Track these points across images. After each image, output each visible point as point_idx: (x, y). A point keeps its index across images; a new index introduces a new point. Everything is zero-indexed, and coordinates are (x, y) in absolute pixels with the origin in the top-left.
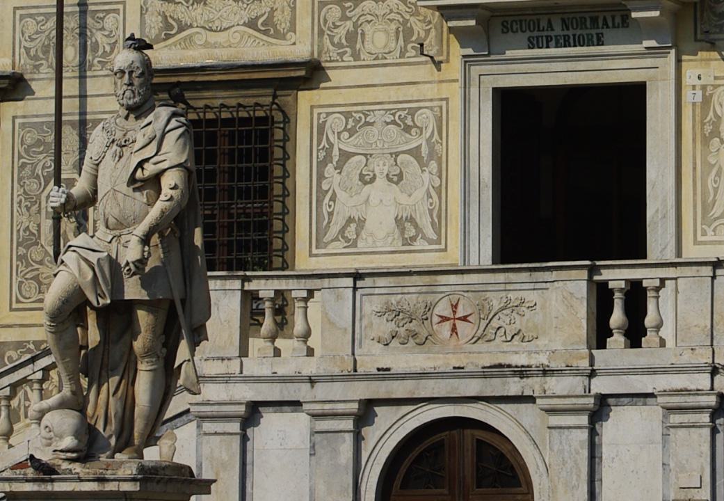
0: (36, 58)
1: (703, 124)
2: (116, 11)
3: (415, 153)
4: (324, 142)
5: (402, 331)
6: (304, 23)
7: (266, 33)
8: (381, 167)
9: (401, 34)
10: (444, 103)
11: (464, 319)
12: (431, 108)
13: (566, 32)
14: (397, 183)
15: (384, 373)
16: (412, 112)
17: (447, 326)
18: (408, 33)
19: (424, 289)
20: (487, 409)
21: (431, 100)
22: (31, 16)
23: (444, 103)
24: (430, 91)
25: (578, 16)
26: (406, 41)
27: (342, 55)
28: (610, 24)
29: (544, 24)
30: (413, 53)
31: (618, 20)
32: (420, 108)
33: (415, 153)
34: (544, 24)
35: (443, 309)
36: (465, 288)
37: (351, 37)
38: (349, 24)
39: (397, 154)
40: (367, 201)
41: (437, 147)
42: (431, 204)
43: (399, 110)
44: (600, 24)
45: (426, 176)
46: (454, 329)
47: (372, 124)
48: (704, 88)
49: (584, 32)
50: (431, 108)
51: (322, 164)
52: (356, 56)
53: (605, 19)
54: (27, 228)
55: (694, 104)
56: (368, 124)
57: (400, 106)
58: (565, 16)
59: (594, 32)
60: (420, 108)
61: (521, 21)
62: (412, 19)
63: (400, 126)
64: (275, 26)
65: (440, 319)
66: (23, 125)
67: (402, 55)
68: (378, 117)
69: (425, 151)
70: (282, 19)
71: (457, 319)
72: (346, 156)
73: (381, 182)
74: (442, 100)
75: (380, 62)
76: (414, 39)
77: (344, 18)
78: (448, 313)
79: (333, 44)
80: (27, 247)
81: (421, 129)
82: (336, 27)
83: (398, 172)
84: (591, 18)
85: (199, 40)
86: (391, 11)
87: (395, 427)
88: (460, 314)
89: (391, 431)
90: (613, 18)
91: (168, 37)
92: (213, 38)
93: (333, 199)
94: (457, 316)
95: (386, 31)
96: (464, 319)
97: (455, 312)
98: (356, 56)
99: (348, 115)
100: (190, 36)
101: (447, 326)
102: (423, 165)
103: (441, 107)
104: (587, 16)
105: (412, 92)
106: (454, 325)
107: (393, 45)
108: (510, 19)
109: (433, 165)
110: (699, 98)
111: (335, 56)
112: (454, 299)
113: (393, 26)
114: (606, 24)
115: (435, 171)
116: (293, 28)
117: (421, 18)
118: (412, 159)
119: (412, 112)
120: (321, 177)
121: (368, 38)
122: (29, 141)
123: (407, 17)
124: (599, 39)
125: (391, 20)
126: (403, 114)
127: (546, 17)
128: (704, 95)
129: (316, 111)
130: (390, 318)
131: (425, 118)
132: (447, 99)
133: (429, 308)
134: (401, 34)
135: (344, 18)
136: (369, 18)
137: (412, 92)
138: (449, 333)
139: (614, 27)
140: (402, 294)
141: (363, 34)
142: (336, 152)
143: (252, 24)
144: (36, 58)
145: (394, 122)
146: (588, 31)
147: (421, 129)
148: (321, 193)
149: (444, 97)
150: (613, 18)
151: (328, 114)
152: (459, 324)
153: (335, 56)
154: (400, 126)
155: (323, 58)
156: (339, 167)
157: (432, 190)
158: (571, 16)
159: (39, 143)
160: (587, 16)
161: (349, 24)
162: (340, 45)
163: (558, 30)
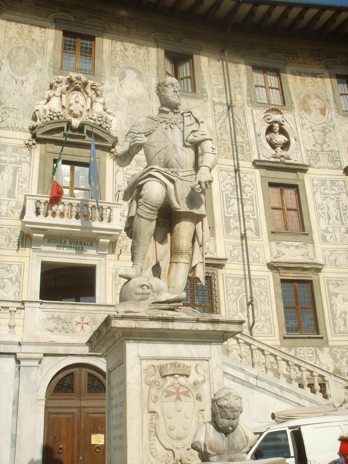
1: (115, 280)
3: (10, 279)
5: (60, 327)
9: (8, 240)
10: (23, 264)
11: (87, 324)
12: (18, 265)
13: (70, 245)
14: (3, 289)
15: (53, 344)
16: (10, 265)
17: (80, 326)
18: (10, 240)
19: (70, 311)
20: (96, 360)
21: (18, 262)
23: (23, 264)
24: (17, 259)
25: (75, 240)
26: (10, 242)
28: (86, 244)
29: (63, 241)
30: (12, 246)
31: (89, 243)
32: (13, 264)
33: (10, 279)
34: (63, 241)
35: (78, 319)
36: (88, 312)
39: (3, 279)
41: (19, 278)
42: (16, 297)
43: (5, 264)
44: (83, 244)
45: (14, 288)
46: (82, 327)
48: (115, 269)
49: (77, 246)
50: (18, 265)
53: (85, 242)
55: (112, 274)
57: (5, 263)
58: (71, 240)
59: (80, 246)
60: (13, 264)
61: (55, 240)
62: (12, 235)
63: (5, 269)
65: (76, 323)
67: (8, 246)
69: (14, 279)
71: (85, 324)
74: (22, 262)
76: (12, 241)
78: (80, 321)
81: (13, 271)
83: (3, 285)
84: (80, 242)
86: (4, 232)
87: (56, 366)
88: (85, 321)
89: (54, 367)
90: (88, 242)
94: (84, 322)
96: (87, 324)
97: (83, 321)
101: (80, 326)
102: (13, 283)
103: (21, 265)
104: (79, 241)
105: (11, 259)
106: (83, 326)
107: (4, 242)
108: (51, 239)
109: (17, 284)
110: (114, 271)
112: (83, 316)
113: (5, 237)
114: (85, 244)
115: (18, 286)
117: (16, 235)
118: (9, 281)
119: (10, 265)
123: (10, 234)
124: (82, 249)
125: (4, 235)
127: (64, 239)
128: (116, 271)
130: (54, 321)
131: (15, 268)
132: (24, 263)
133: (72, 319)
134: (8, 240)
137: (11, 259)
138: (80, 329)
139: (88, 245)
140: (60, 312)
145: (3, 268)
146: (78, 246)
147: (13, 271)
149: (23, 261)
150: (88, 242)
152: (85, 325)
154: (5, 269)
157: (16, 293)
158: (73, 240)
160: (79, 241)
163: (68, 243)
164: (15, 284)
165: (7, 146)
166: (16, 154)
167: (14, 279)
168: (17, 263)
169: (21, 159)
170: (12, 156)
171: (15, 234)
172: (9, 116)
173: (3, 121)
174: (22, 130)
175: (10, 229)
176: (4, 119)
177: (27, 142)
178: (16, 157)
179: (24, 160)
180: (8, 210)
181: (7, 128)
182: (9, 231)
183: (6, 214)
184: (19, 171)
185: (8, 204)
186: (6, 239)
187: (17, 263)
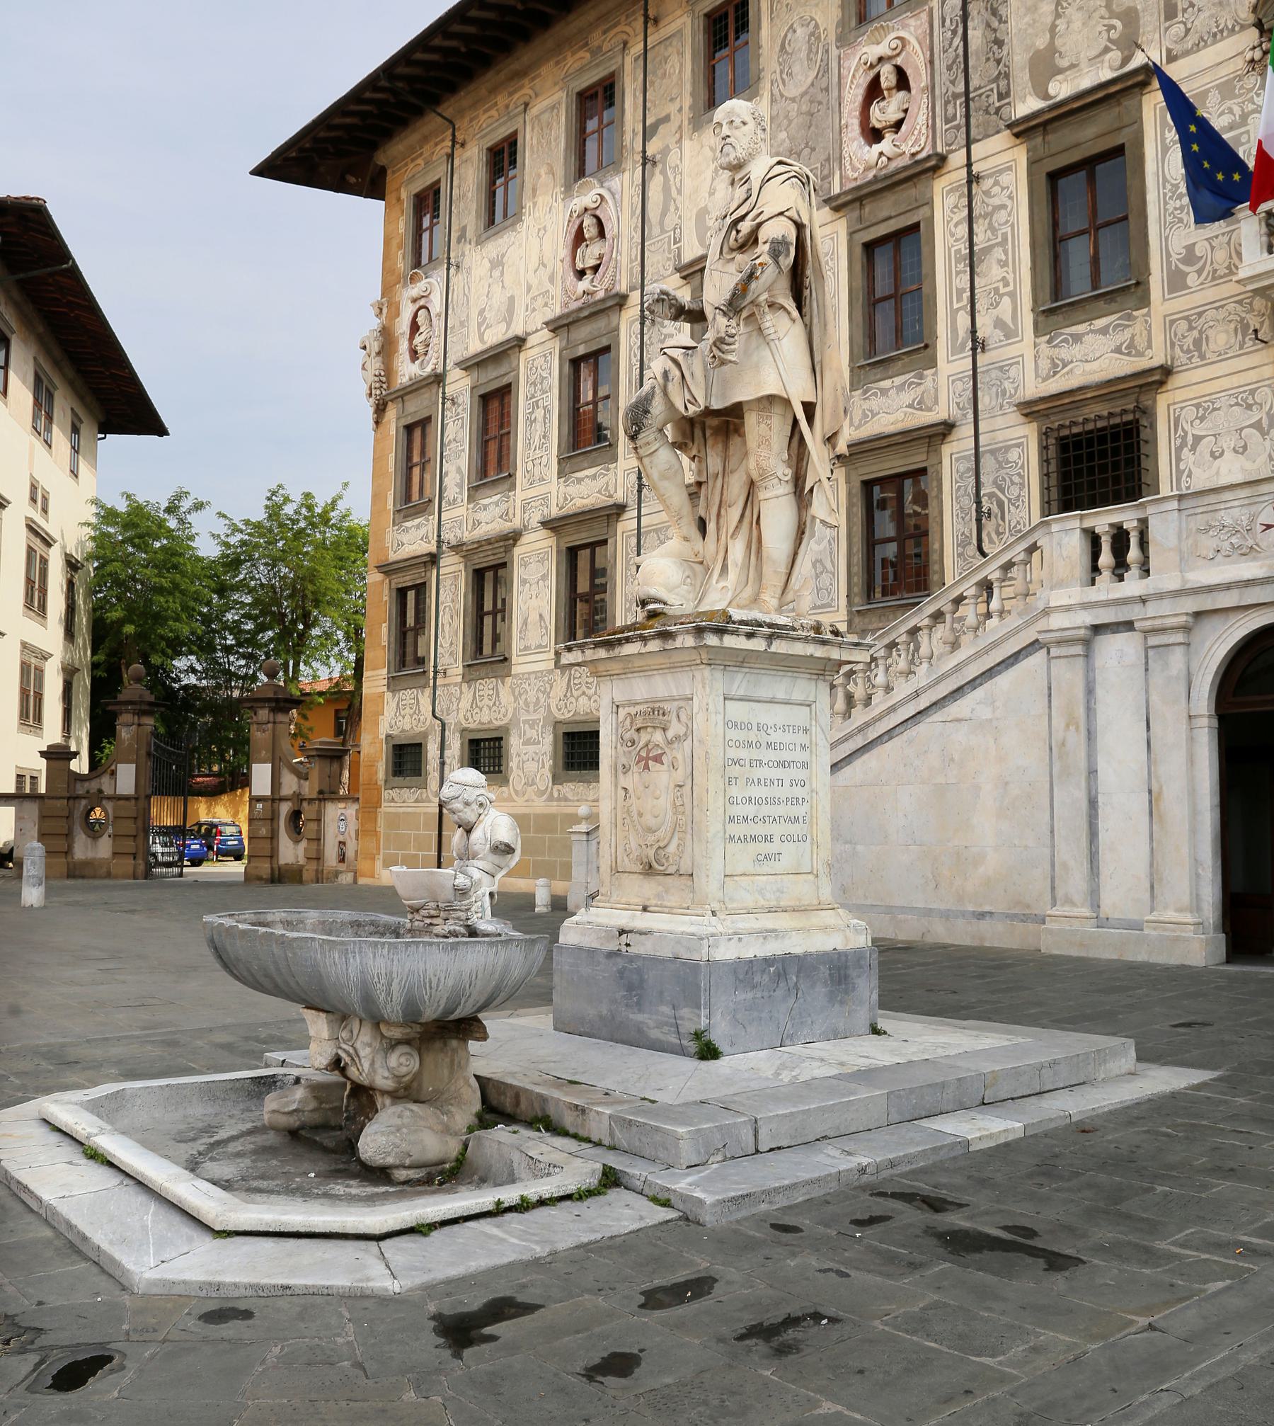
0: (963, 409)
2: (1018, 363)
3: (1257, 426)
4: (1180, 432)
6: (1158, 339)
7: (1128, 354)
8: (1228, 442)
16: (1252, 392)
22: (960, 379)
26: (1244, 336)
27: (1190, 359)
33: (1257, 426)
37: (1197, 343)
38: (1195, 333)
39: (1241, 429)
40: (1218, 473)
47: (1218, 409)
50: (1269, 386)
51: (1179, 450)
52: (1202, 357)
54: (963, 534)
56: (1215, 409)
62: (1248, 316)
64: (1135, 348)
66: (958, 459)
67: (1241, 348)
68: (1223, 402)
69: (1265, 423)
70: (1141, 342)
72: (1198, 439)
73: (1228, 455)
75: (1222, 357)
77: (1191, 328)
79: (1182, 350)
80: (964, 547)
81: (1261, 405)
82: (1184, 337)
85: (1078, 372)
91: (1055, 373)
92: (1088, 367)
93: (1189, 476)
95: (1227, 332)
98: (1202, 357)
99: (1198, 406)
100: (1071, 370)
105: (1252, 376)
107: (1233, 341)
111: (1185, 361)
113: (1232, 326)
116: (1150, 346)
119: (1252, 392)
120: (1179, 459)
121: (1211, 340)
122: (962, 469)
126: (1244, 395)
129: (1172, 408)
135: (1191, 328)
136: (1211, 323)
137: (1252, 376)
141: (1207, 338)
142: (1190, 438)
143: (1118, 350)
144: (963, 409)
145: (1237, 404)
148: (1180, 473)
151: (1182, 408)
153: (1185, 361)
155: (1176, 364)
156: (1193, 449)
159: (968, 470)
161: (1195, 333)
162: (1188, 351)
164: (1268, 433)
165: (1208, 91)
166: (1229, 103)
167: (1265, 423)
168: (1267, 383)
169: (1243, 110)
170: (1222, 114)
171: (1253, 310)
172: (1199, 10)
173: (1188, 31)
174: (1237, 28)
175: (1240, 302)
176: (1189, 26)
177: (1249, 57)
178: (1231, 111)
179: (1251, 107)
180: (1231, 257)
181: (1202, 44)
182: (1239, 308)
183: (1229, 267)
184: (1243, 144)
185: (1229, 243)
186: (1236, 329)
187: (1267, 383)
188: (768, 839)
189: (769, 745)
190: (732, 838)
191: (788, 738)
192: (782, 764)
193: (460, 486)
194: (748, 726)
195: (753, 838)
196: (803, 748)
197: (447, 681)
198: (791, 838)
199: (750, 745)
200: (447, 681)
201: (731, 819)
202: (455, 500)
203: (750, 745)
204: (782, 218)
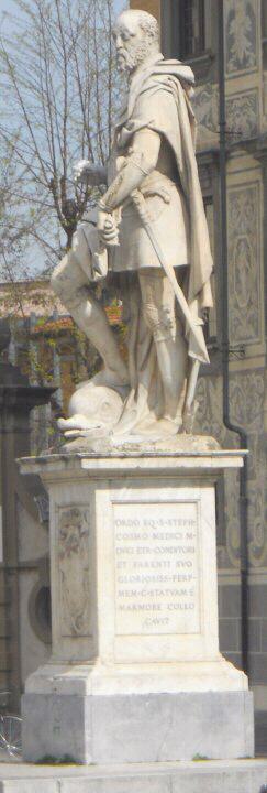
188: (156, 607)
189: (155, 536)
190: (121, 608)
191: (173, 529)
192: (168, 550)
193: (250, 36)
194: (134, 523)
195: (141, 607)
196: (189, 536)
197: (247, 365)
198: (179, 607)
199: (137, 537)
200: (247, 365)
201: (121, 593)
202: (246, 60)
203: (137, 537)
204: (146, 129)
